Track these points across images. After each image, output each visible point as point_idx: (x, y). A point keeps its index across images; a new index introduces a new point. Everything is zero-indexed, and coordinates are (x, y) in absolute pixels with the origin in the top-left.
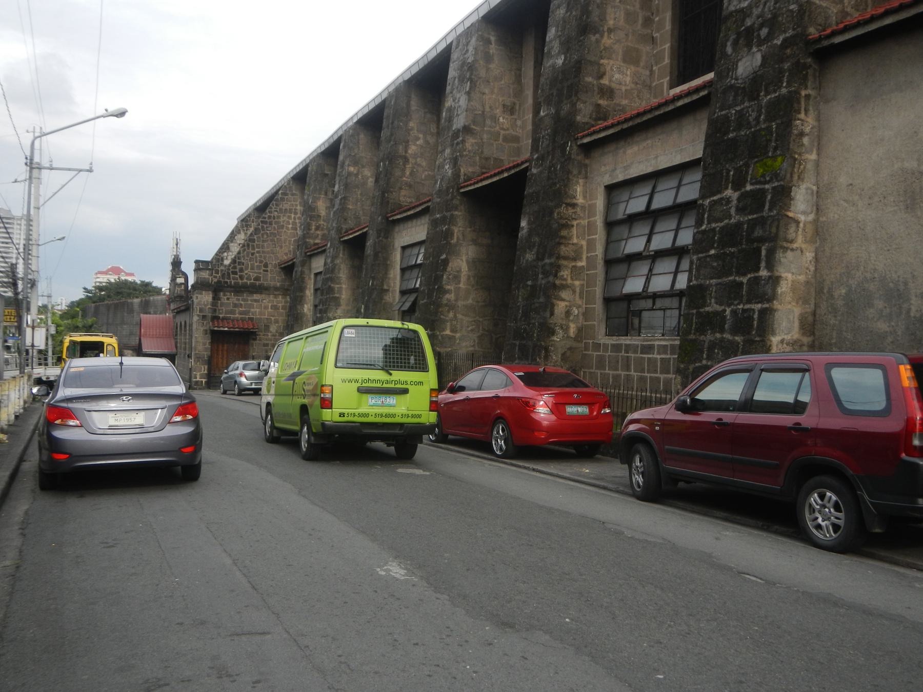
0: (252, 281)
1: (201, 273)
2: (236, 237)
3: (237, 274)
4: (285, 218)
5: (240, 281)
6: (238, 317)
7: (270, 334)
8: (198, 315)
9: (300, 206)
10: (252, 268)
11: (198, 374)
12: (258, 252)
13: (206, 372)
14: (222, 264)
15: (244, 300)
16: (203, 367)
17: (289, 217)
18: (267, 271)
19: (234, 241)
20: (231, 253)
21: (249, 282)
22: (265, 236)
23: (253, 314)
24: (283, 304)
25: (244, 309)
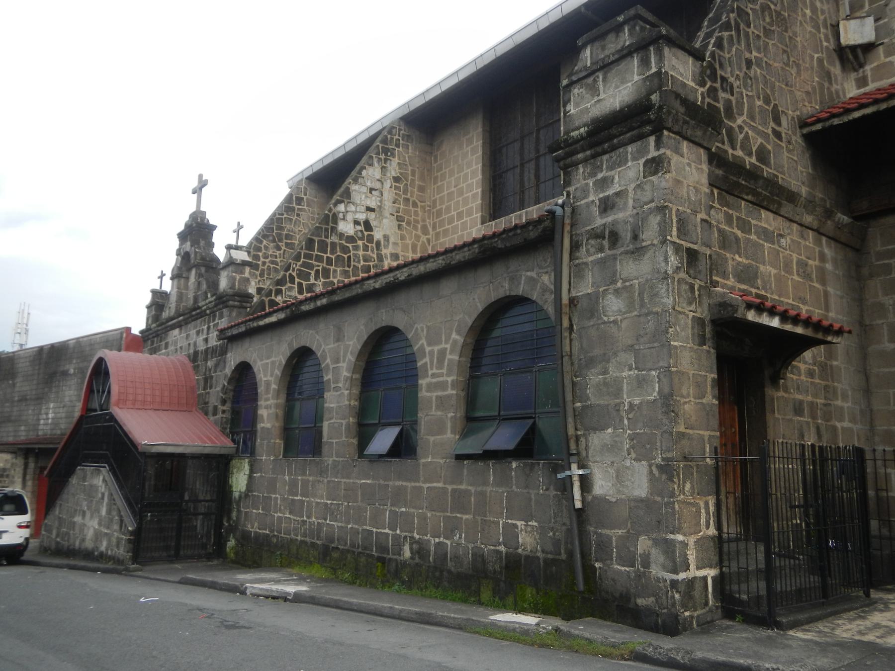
1: (674, 61)
2: (364, 173)
5: (730, 151)
7: (803, 367)
8: (677, 248)
10: (752, 117)
11: (691, 540)
13: (712, 531)
14: (334, 229)
15: (745, 226)
16: (702, 504)
18: (778, 135)
19: (360, 180)
20: (352, 208)
21: (747, 159)
22: (768, 20)
23: (764, 288)
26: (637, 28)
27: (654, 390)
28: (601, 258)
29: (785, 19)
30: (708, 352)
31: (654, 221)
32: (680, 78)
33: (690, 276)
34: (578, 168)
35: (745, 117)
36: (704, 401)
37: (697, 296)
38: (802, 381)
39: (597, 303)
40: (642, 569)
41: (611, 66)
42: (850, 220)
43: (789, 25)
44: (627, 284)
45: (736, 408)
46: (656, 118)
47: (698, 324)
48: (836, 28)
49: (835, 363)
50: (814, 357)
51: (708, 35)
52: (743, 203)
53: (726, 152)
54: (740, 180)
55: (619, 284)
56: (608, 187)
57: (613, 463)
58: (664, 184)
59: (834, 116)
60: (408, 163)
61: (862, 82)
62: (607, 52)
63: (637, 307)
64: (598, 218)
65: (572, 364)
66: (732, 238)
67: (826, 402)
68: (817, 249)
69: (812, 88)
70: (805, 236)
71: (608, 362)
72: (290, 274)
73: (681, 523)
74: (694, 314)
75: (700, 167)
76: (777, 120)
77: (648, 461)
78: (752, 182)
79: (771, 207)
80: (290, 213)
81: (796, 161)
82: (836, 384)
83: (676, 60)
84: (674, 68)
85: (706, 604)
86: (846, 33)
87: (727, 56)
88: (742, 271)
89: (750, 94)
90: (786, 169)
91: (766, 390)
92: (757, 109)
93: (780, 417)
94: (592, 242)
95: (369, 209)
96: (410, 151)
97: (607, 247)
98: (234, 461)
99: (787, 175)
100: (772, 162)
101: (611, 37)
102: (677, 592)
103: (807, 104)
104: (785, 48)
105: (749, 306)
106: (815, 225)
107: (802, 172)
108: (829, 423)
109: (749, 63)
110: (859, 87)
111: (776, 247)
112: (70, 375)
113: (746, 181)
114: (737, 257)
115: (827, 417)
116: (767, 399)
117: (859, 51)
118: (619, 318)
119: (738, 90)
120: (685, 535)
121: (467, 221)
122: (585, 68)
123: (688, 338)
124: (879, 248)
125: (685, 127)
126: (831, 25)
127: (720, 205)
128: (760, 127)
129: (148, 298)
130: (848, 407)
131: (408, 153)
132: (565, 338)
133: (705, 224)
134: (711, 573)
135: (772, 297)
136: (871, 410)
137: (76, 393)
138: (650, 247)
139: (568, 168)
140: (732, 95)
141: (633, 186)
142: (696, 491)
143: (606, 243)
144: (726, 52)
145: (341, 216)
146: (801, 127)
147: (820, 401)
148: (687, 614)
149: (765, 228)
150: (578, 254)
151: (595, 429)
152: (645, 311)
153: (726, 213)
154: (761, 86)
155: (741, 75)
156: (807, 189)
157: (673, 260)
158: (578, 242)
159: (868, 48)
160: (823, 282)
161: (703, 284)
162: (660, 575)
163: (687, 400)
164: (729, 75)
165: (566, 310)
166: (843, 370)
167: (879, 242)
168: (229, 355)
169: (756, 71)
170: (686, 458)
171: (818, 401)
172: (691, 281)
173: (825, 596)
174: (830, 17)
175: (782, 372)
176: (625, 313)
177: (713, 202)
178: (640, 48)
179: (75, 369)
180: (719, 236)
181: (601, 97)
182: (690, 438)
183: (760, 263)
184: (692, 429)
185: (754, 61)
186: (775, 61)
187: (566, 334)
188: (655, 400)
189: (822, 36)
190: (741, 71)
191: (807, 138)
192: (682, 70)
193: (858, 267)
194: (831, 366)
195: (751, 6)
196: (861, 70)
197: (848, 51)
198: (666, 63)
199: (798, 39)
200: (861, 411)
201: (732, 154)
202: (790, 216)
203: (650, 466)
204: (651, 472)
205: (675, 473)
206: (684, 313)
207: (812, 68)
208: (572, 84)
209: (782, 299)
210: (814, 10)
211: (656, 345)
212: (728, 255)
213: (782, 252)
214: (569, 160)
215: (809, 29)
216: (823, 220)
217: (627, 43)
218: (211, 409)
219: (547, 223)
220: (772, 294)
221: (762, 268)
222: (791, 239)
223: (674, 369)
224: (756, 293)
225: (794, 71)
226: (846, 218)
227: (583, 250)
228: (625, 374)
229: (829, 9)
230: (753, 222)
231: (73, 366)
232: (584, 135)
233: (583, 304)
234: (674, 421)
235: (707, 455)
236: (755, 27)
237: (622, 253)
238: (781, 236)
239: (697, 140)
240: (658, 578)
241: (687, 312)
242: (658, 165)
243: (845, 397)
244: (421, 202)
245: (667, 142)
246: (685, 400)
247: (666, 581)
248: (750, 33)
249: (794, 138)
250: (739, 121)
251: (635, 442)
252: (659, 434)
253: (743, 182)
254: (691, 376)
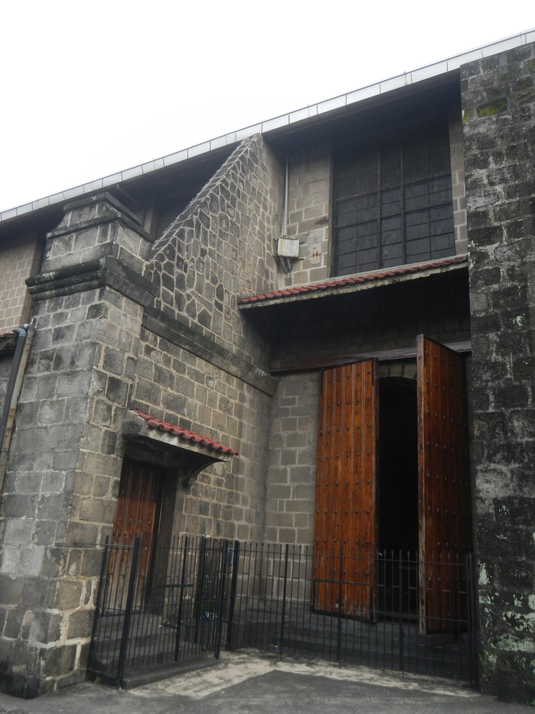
0: (196, 321)
1: (126, 238)
3: (172, 290)
4: (252, 206)
5: (177, 311)
6: (161, 412)
7: (212, 477)
8: (101, 377)
9: (271, 197)
10: (199, 290)
11: (67, 615)
12: (212, 253)
13: (91, 606)
15: (180, 367)
16: (84, 583)
17: (257, 208)
18: (220, 307)
21: (190, 319)
22: (224, 226)
23: (189, 415)
24: (237, 401)
25: (174, 393)
26: (104, 208)
27: (61, 486)
28: (47, 376)
29: (238, 227)
30: (115, 459)
31: (87, 352)
32: (129, 251)
33: (109, 399)
34: (45, 302)
35: (193, 289)
36: (104, 498)
37: (112, 415)
38: (210, 488)
39: (36, 410)
40: (22, 639)
41: (82, 231)
42: (266, 374)
43: (240, 233)
44: (60, 399)
45: (155, 505)
46: (102, 276)
47: (110, 437)
48: (276, 242)
49: (240, 476)
50: (224, 470)
51: (177, 226)
52: (182, 350)
53: (173, 311)
54: (180, 334)
55: (54, 399)
56: (62, 321)
57: (20, 546)
58: (98, 326)
59: (259, 300)
61: (288, 282)
62: (82, 220)
63: (63, 417)
64: (51, 344)
65: (8, 459)
66: (168, 375)
67: (229, 505)
68: (239, 392)
69: (252, 279)
70: (230, 381)
71: (34, 460)
73: (59, 599)
74: (107, 429)
75: (134, 318)
76: (220, 295)
77: (46, 545)
78: (190, 336)
79: (204, 357)
81: (231, 327)
82: (239, 492)
83: (128, 238)
84: (125, 243)
85: (71, 668)
86: (282, 247)
87: (186, 244)
88: (172, 400)
89: (200, 273)
90: (222, 331)
91: (177, 492)
92: (205, 285)
93: (186, 514)
94: (43, 361)
97: (52, 367)
99: (222, 335)
100: (212, 324)
101: (86, 210)
102: (43, 659)
103: (246, 289)
104: (235, 248)
105: (151, 428)
106: (239, 374)
107: (235, 335)
108: (228, 521)
109: (203, 253)
110: (286, 285)
111: (205, 386)
113: (184, 335)
114: (169, 389)
115: (227, 516)
116: (177, 500)
117: (288, 261)
118: (49, 425)
119: (191, 269)
120: (61, 609)
121: (7, 329)
122: (66, 228)
123: (97, 447)
124: (284, 397)
125: (124, 287)
126: (274, 239)
127: (161, 349)
128: (205, 298)
130: (246, 510)
132: (7, 436)
133: (131, 362)
134: (81, 642)
135: (195, 422)
136: (265, 513)
138: (81, 372)
139: (38, 300)
140: (186, 271)
141: (79, 323)
142: (80, 572)
143: (52, 364)
144: (186, 240)
146: (239, 304)
147: (224, 504)
148: (49, 678)
149: (197, 371)
150: (31, 370)
151: (13, 516)
152: (68, 422)
153: (165, 356)
154: (211, 269)
155: (196, 259)
156: (237, 348)
157: (96, 385)
158: (33, 360)
159: (294, 260)
160: (240, 416)
161: (120, 406)
162: (34, 645)
163: (87, 496)
164: (185, 257)
165: (12, 413)
166: (246, 482)
167: (284, 392)
169: (208, 258)
170: (75, 544)
171: (222, 504)
172: (109, 403)
173: (176, 659)
174: (274, 235)
175: (191, 479)
176: (54, 422)
177: (155, 346)
178: (103, 223)
180: (156, 371)
181: (71, 252)
182: (83, 527)
183: (189, 396)
184: (87, 520)
185: (208, 251)
186: (225, 254)
187: (8, 434)
188: (60, 495)
189: (266, 246)
190: (196, 256)
191: (243, 312)
192: (132, 246)
193: (270, 408)
194: (237, 478)
195: (212, 214)
196: (289, 274)
197: (281, 259)
198: (118, 238)
199: (247, 244)
200: (257, 514)
201: (178, 314)
202: (220, 365)
203: (46, 549)
204: (45, 555)
205: (62, 556)
206: (98, 427)
207: (255, 266)
208: (54, 237)
209: (203, 425)
210: (262, 227)
211: (70, 450)
212: (161, 387)
213: (209, 391)
214: (39, 295)
215: (256, 238)
216: (246, 371)
217: (96, 217)
219: (11, 341)
220: (195, 420)
221: (190, 400)
222: (219, 382)
223: (78, 471)
224: (181, 418)
225: (240, 265)
226: (263, 372)
227: (36, 366)
228: (44, 471)
229: (274, 229)
230: (188, 365)
232: (52, 277)
233: (26, 410)
234: (71, 513)
235: (98, 542)
236: (212, 228)
237: (61, 374)
238: (211, 379)
239: (135, 298)
240: (32, 647)
241: (101, 427)
242: (98, 311)
243: (245, 502)
245: (107, 296)
246: (84, 496)
247: (36, 649)
248: (208, 232)
249: (232, 311)
250: (189, 291)
251: (40, 528)
252: (58, 523)
253: (183, 335)
254: (94, 477)
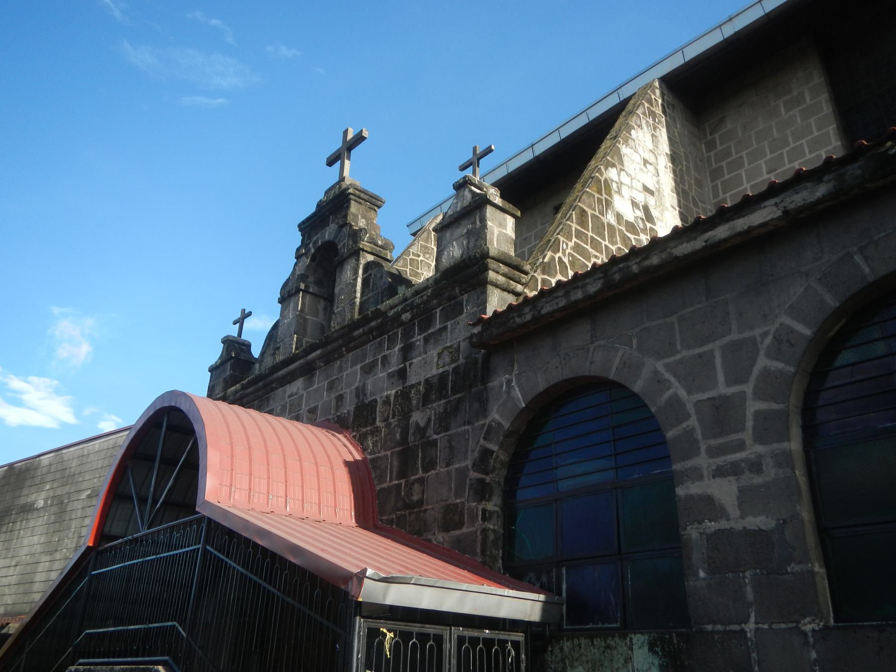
14: (609, 204)
60: (679, 142)
72: (559, 258)
80: (427, 256)
95: (646, 189)
96: (678, 126)
98: (567, 645)
112: (37, 509)
129: (214, 353)
131: (677, 128)
137: (43, 540)
145: (614, 186)
168: (498, 381)
179: (46, 500)
218: (433, 511)
231: (43, 495)
244: (701, 202)
